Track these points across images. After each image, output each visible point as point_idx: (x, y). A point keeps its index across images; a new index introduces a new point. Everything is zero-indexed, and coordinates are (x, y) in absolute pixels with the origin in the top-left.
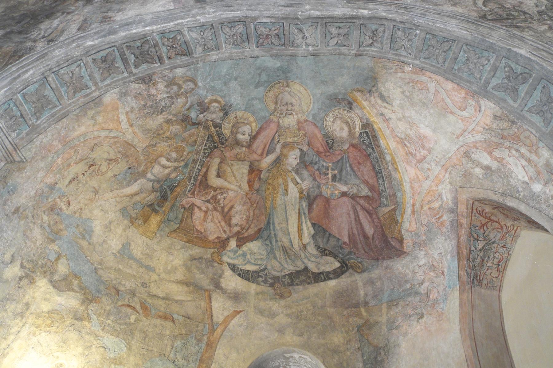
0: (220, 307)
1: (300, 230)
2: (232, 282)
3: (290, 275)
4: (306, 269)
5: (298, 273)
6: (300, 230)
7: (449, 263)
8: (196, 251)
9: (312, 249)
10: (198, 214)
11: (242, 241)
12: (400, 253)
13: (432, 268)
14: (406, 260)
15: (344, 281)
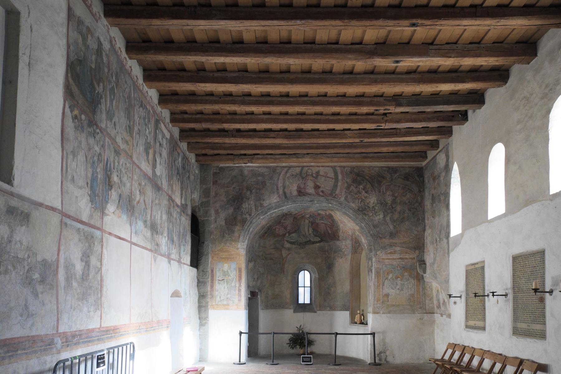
0: (284, 253)
1: (308, 230)
2: (287, 245)
3: (305, 242)
4: (310, 240)
5: (308, 241)
6: (308, 230)
7: (350, 246)
8: (277, 239)
9: (312, 235)
10: (277, 229)
11: (290, 233)
12: (338, 240)
13: (346, 246)
14: (340, 242)
15: (322, 244)
